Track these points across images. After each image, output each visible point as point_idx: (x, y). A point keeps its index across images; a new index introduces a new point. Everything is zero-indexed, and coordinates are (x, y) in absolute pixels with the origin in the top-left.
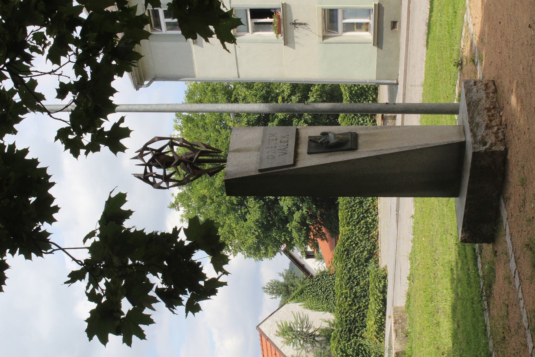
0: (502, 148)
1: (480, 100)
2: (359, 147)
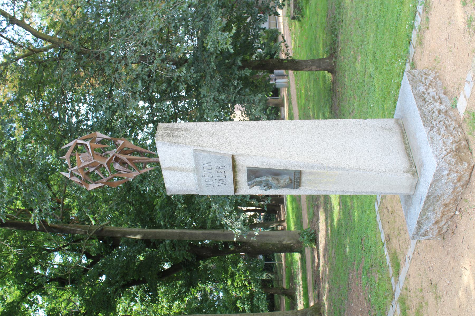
2: (302, 184)
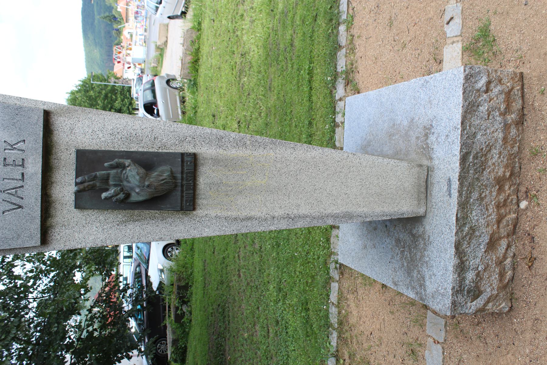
0: (504, 306)
1: (490, 150)
2: (201, 201)
